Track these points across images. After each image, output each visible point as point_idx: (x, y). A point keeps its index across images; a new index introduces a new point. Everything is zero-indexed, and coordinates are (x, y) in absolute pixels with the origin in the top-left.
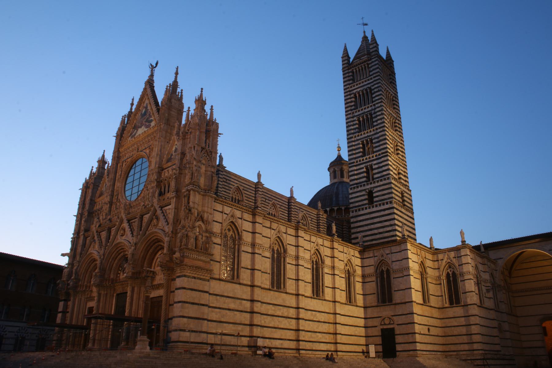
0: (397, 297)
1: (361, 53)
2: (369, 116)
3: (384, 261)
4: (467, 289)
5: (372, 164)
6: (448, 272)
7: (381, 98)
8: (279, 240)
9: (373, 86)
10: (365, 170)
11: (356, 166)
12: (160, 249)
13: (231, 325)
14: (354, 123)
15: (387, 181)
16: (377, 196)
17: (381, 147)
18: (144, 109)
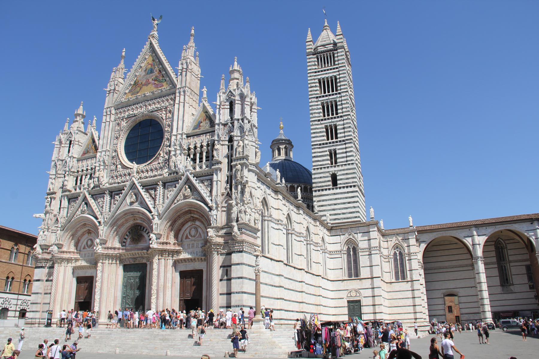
0: (364, 272)
1: (324, 41)
2: (334, 103)
3: (350, 239)
4: (413, 267)
5: (336, 149)
6: (395, 252)
7: (347, 88)
8: (289, 217)
9: (339, 75)
10: (328, 153)
11: (319, 148)
12: (189, 221)
13: (267, 299)
14: (319, 107)
15: (351, 166)
16: (341, 179)
17: (346, 134)
18: (150, 66)
